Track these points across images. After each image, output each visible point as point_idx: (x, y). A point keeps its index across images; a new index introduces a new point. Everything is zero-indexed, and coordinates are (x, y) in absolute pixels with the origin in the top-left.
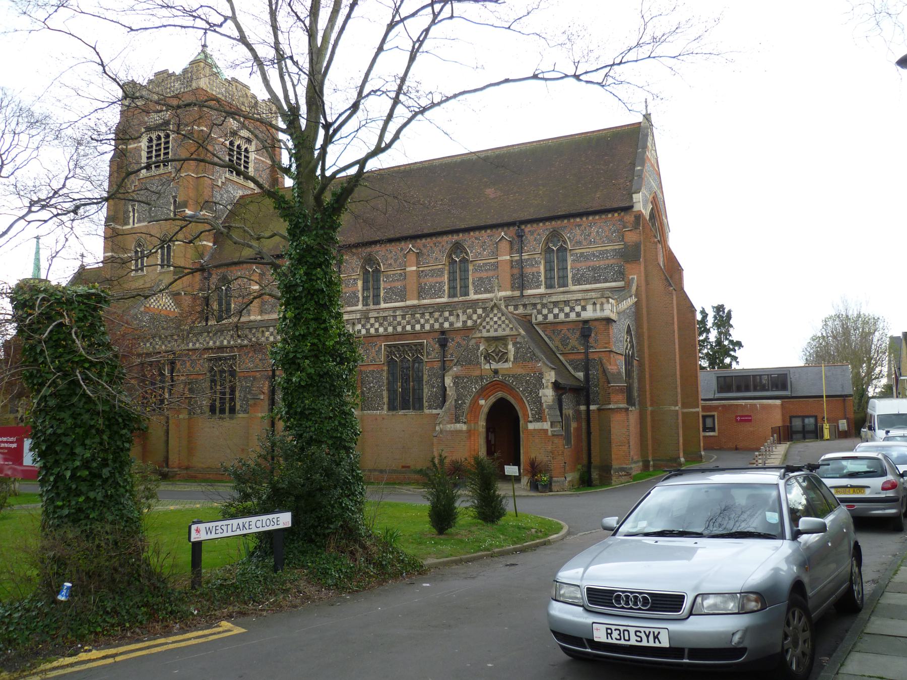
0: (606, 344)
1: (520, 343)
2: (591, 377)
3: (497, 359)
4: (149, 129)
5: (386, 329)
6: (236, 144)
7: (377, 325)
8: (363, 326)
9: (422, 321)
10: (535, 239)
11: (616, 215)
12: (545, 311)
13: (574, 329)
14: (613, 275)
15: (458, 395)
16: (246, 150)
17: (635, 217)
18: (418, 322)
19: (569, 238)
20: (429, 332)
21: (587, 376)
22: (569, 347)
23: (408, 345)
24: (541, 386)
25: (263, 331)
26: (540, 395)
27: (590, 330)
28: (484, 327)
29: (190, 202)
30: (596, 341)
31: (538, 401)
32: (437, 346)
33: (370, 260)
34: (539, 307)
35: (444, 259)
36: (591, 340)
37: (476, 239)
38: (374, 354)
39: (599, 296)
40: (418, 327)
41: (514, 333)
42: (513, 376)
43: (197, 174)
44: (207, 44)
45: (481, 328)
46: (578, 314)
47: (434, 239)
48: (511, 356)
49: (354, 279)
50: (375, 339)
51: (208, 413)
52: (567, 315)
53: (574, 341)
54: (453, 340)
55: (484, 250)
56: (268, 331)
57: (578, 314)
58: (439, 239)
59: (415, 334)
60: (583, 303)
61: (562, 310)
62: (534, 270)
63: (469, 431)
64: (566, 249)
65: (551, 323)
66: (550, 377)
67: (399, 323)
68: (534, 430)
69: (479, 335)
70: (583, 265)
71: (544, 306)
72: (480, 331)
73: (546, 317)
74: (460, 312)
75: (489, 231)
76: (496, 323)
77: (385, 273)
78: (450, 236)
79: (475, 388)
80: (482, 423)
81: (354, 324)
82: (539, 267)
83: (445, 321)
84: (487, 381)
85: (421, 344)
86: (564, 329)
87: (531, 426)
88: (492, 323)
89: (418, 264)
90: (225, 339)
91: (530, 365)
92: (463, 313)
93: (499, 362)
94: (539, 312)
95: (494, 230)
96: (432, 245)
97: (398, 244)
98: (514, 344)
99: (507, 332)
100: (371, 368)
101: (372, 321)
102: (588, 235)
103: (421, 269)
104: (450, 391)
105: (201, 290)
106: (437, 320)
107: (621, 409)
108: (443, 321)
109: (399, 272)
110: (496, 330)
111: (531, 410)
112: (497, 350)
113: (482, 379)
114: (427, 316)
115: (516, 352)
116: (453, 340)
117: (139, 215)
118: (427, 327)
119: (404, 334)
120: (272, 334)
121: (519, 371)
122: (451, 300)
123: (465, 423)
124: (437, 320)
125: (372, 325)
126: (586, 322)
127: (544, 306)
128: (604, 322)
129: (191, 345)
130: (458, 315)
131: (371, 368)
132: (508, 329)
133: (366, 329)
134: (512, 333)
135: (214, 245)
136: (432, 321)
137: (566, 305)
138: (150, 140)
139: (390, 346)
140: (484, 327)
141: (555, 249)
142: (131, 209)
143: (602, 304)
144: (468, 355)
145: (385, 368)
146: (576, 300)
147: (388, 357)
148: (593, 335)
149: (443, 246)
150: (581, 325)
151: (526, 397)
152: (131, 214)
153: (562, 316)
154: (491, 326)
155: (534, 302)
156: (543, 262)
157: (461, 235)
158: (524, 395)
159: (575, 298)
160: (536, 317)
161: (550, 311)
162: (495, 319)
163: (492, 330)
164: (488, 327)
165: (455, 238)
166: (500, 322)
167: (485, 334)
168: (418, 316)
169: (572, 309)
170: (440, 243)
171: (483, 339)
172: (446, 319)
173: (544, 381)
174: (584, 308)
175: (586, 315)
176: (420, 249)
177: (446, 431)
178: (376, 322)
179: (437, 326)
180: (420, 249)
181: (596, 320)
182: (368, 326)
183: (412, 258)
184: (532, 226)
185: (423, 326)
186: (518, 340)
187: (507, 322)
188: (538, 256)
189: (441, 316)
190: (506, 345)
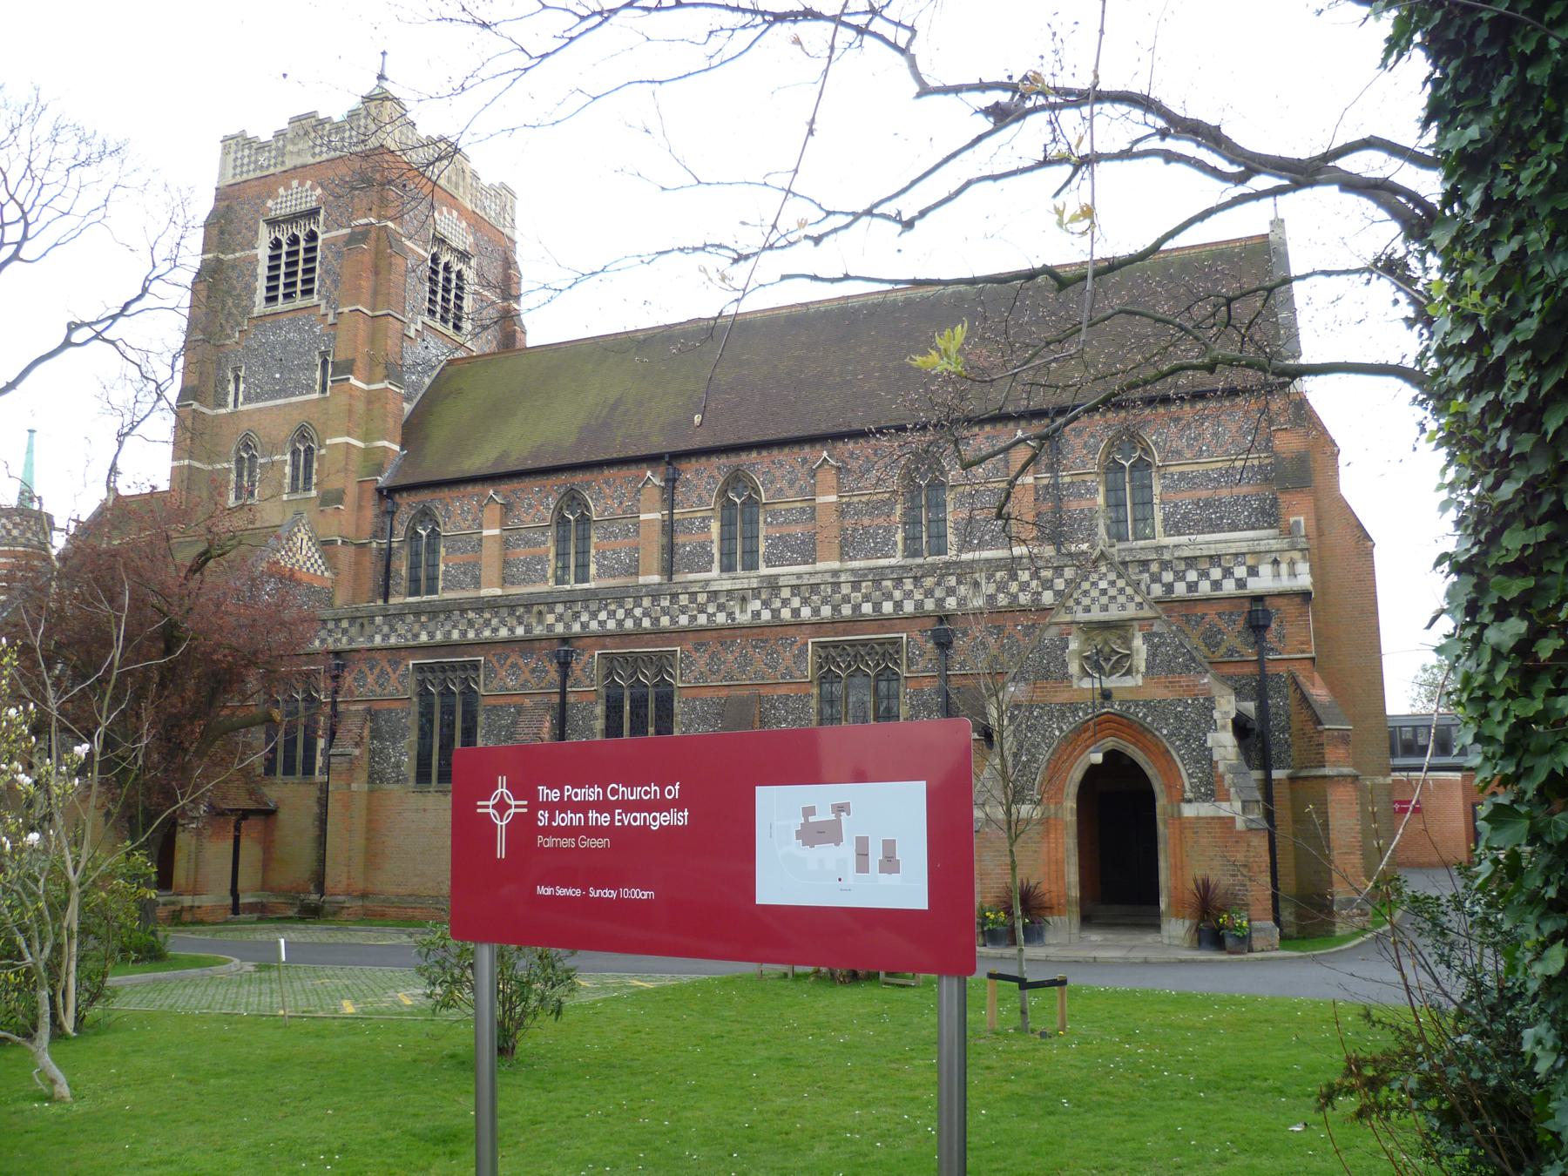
0: (1302, 643)
1: (1160, 635)
2: (1273, 710)
3: (1107, 667)
4: (273, 223)
5: (816, 611)
6: (444, 259)
7: (796, 602)
8: (766, 604)
9: (897, 595)
10: (1085, 445)
12: (1168, 577)
13: (1231, 614)
14: (1250, 516)
16: (459, 275)
18: (889, 597)
19: (1156, 443)
20: (913, 617)
21: (1262, 708)
22: (1223, 650)
23: (864, 643)
24: (1211, 725)
25: (540, 613)
26: (1209, 744)
27: (1268, 615)
29: (359, 364)
30: (1281, 638)
31: (1205, 757)
32: (930, 645)
33: (736, 479)
34: (1154, 567)
35: (894, 482)
36: (1271, 636)
38: (790, 663)
39: (1285, 546)
40: (888, 607)
42: (1146, 704)
43: (373, 310)
44: (387, 74)
45: (1071, 603)
46: (1241, 584)
48: (1140, 662)
49: (704, 519)
50: (792, 630)
51: (412, 782)
52: (1216, 585)
53: (1233, 637)
54: (965, 633)
56: (552, 611)
57: (1241, 584)
59: (881, 621)
60: (1250, 561)
61: (1204, 574)
62: (1085, 504)
63: (1045, 821)
64: (1149, 465)
65: (1182, 601)
66: (1227, 706)
67: (846, 599)
68: (1198, 818)
69: (1068, 618)
70: (1186, 498)
71: (1165, 565)
73: (1169, 588)
74: (981, 577)
75: (988, 428)
76: (1104, 592)
77: (768, 508)
79: (1061, 730)
80: (1070, 804)
81: (744, 599)
82: (1094, 499)
83: (948, 595)
85: (895, 642)
86: (1211, 614)
87: (1189, 811)
88: (1095, 593)
89: (839, 489)
90: (454, 627)
91: (1184, 681)
92: (988, 579)
93: (1111, 674)
94: (1156, 579)
95: (999, 426)
97: (796, 450)
98: (1147, 638)
99: (1131, 611)
100: (782, 691)
101: (786, 593)
102: (1195, 439)
103: (844, 500)
105: (375, 536)
106: (929, 593)
107: (1345, 776)
108: (943, 595)
109: (799, 505)
110: (1105, 608)
111: (1190, 776)
112: (1107, 649)
113: (1074, 712)
114: (908, 584)
115: (1152, 655)
116: (965, 633)
117: (248, 387)
118: (909, 607)
119: (856, 621)
120: (560, 618)
121: (1160, 693)
122: (910, 561)
124: (929, 593)
125: (785, 602)
126: (1258, 599)
127: (1165, 565)
128: (1298, 600)
129: (378, 639)
130: (976, 584)
131: (782, 691)
132: (1131, 608)
133: (773, 611)
134: (1141, 614)
135: (402, 450)
137: (1213, 565)
138: (277, 244)
139: (823, 645)
140: (1078, 603)
141: (1127, 465)
142: (231, 376)
143: (1292, 563)
144: (1042, 659)
145: (815, 691)
146: (1236, 555)
147: (821, 667)
148: (1273, 626)
150: (1247, 606)
151: (1178, 749)
152: (231, 388)
153: (1205, 588)
154: (1093, 600)
155: (1143, 558)
156: (1101, 489)
158: (1172, 743)
159: (1233, 551)
160: (1148, 587)
161: (1180, 576)
162: (1103, 585)
163: (1095, 608)
164: (1086, 601)
166: (1112, 592)
167: (1081, 616)
168: (888, 583)
169: (1228, 573)
171: (1074, 628)
172: (951, 592)
173: (1216, 715)
174: (1253, 571)
175: (1256, 585)
176: (843, 462)
178: (793, 595)
179: (930, 605)
180: (843, 462)
181: (1281, 595)
182: (777, 604)
183: (829, 477)
185: (898, 605)
186: (1155, 629)
187: (1129, 591)
188: (1092, 477)
189: (938, 584)
190: (1127, 642)
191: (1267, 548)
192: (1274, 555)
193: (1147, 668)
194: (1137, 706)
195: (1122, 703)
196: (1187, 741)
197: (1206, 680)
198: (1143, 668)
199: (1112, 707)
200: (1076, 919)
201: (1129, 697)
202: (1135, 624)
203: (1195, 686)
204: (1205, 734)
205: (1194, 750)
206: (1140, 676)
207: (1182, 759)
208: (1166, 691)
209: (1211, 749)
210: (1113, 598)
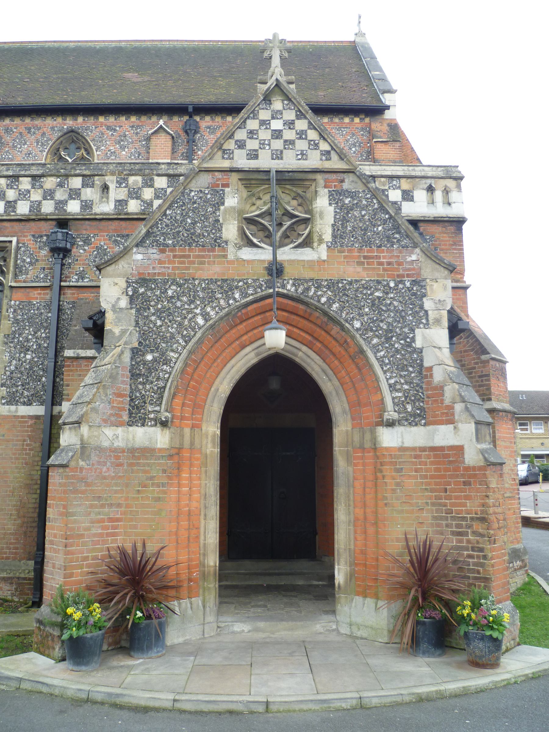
1: (353, 195)
11: (357, 120)
15: (143, 335)
17: (389, 125)
26: (418, 344)
28: (241, 145)
32: (44, 252)
37: (109, 128)
41: (335, 163)
42: (332, 285)
45: (230, 145)
47: (28, 120)
54: (87, 241)
55: (123, 148)
58: (38, 122)
60: (405, 185)
68: (402, 449)
69: (226, 164)
72: (228, 154)
74: (111, 181)
75: (133, 119)
76: (277, 134)
78: (59, 119)
79: (206, 317)
83: (71, 198)
84: (244, 295)
88: (264, 135)
91: (385, 256)
92: (119, 183)
95: (144, 118)
96: (22, 129)
104: (118, 320)
108: (65, 197)
110: (278, 155)
113: (228, 293)
116: (87, 241)
123: (164, 424)
124: (49, 194)
130: (105, 188)
134: (328, 165)
136: (36, 196)
140: (241, 145)
143: (446, 192)
144: (184, 216)
149: (44, 134)
151: (375, 349)
154: (262, 144)
157: (80, 119)
158: (368, 341)
159: (389, 173)
162: (276, 125)
164: (252, 145)
165: (69, 123)
166: (289, 135)
170: (39, 129)
171: (234, 178)
172: (75, 194)
173: (428, 304)
174: (408, 196)
177: (100, 449)
179: (48, 207)
181: (436, 221)
184: (213, 120)
189: (61, 185)
191: (423, 174)
192: (429, 181)
193: (334, 236)
194: (318, 287)
195: (297, 282)
196: (388, 339)
197: (414, 257)
198: (328, 237)
199: (283, 286)
200: (212, 598)
201: (308, 274)
202: (319, 177)
203: (400, 264)
204: (412, 330)
205: (397, 351)
206: (324, 246)
207: (380, 361)
208: (359, 269)
209: (421, 351)
210: (290, 143)
